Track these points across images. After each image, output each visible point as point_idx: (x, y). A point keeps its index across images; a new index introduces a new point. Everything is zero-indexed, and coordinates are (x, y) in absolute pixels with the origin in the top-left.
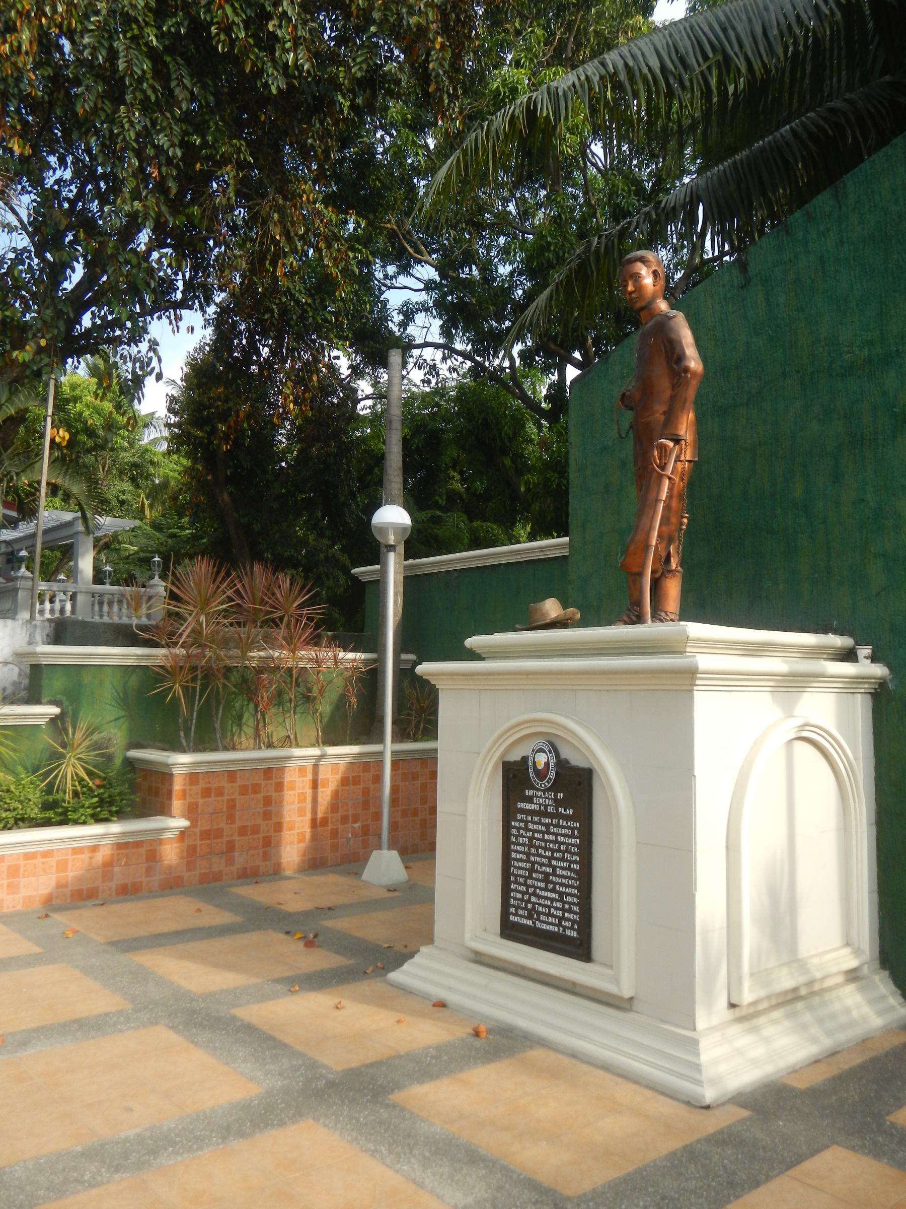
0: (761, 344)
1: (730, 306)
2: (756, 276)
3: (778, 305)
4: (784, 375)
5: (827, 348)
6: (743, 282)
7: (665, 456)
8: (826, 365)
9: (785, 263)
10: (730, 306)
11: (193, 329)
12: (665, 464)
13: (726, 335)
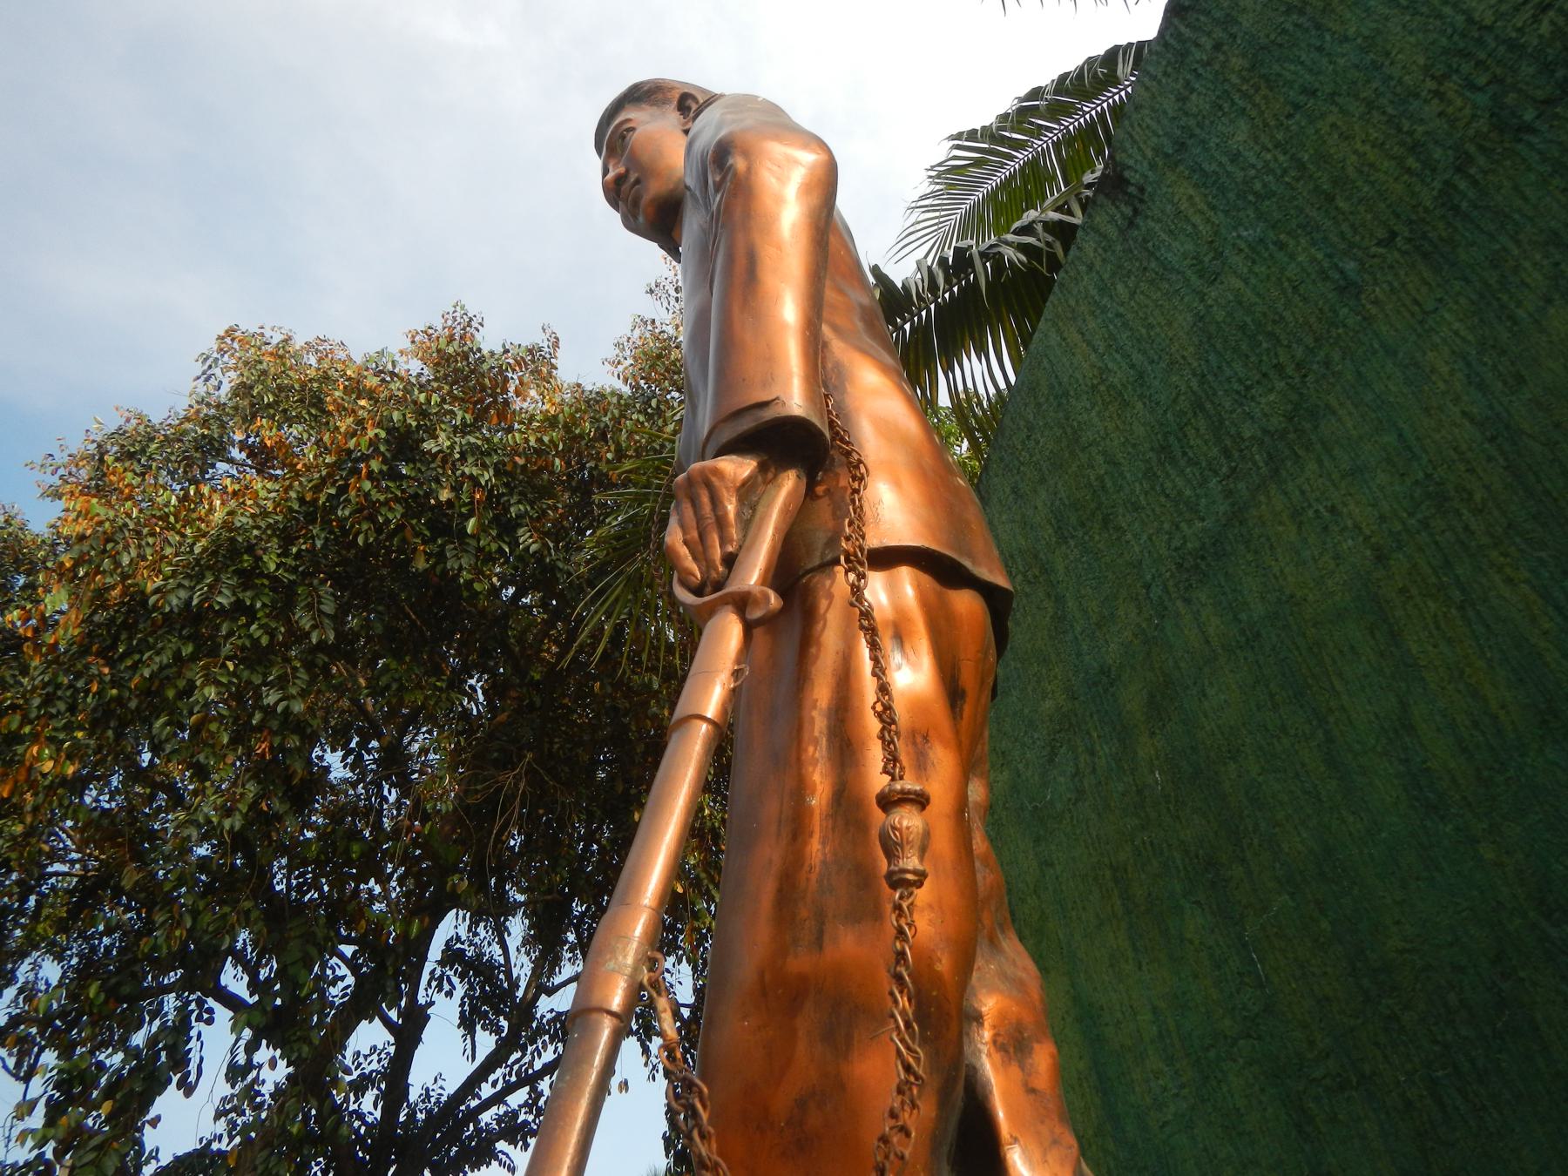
0: (1238, 284)
1: (1120, 287)
2: (1153, 166)
3: (1235, 158)
4: (1348, 288)
5: (1450, 87)
6: (1128, 211)
7: (721, 523)
8: (1482, 124)
9: (1209, 63)
10: (1120, 287)
11: (626, 1083)
12: (730, 561)
13: (1137, 358)
